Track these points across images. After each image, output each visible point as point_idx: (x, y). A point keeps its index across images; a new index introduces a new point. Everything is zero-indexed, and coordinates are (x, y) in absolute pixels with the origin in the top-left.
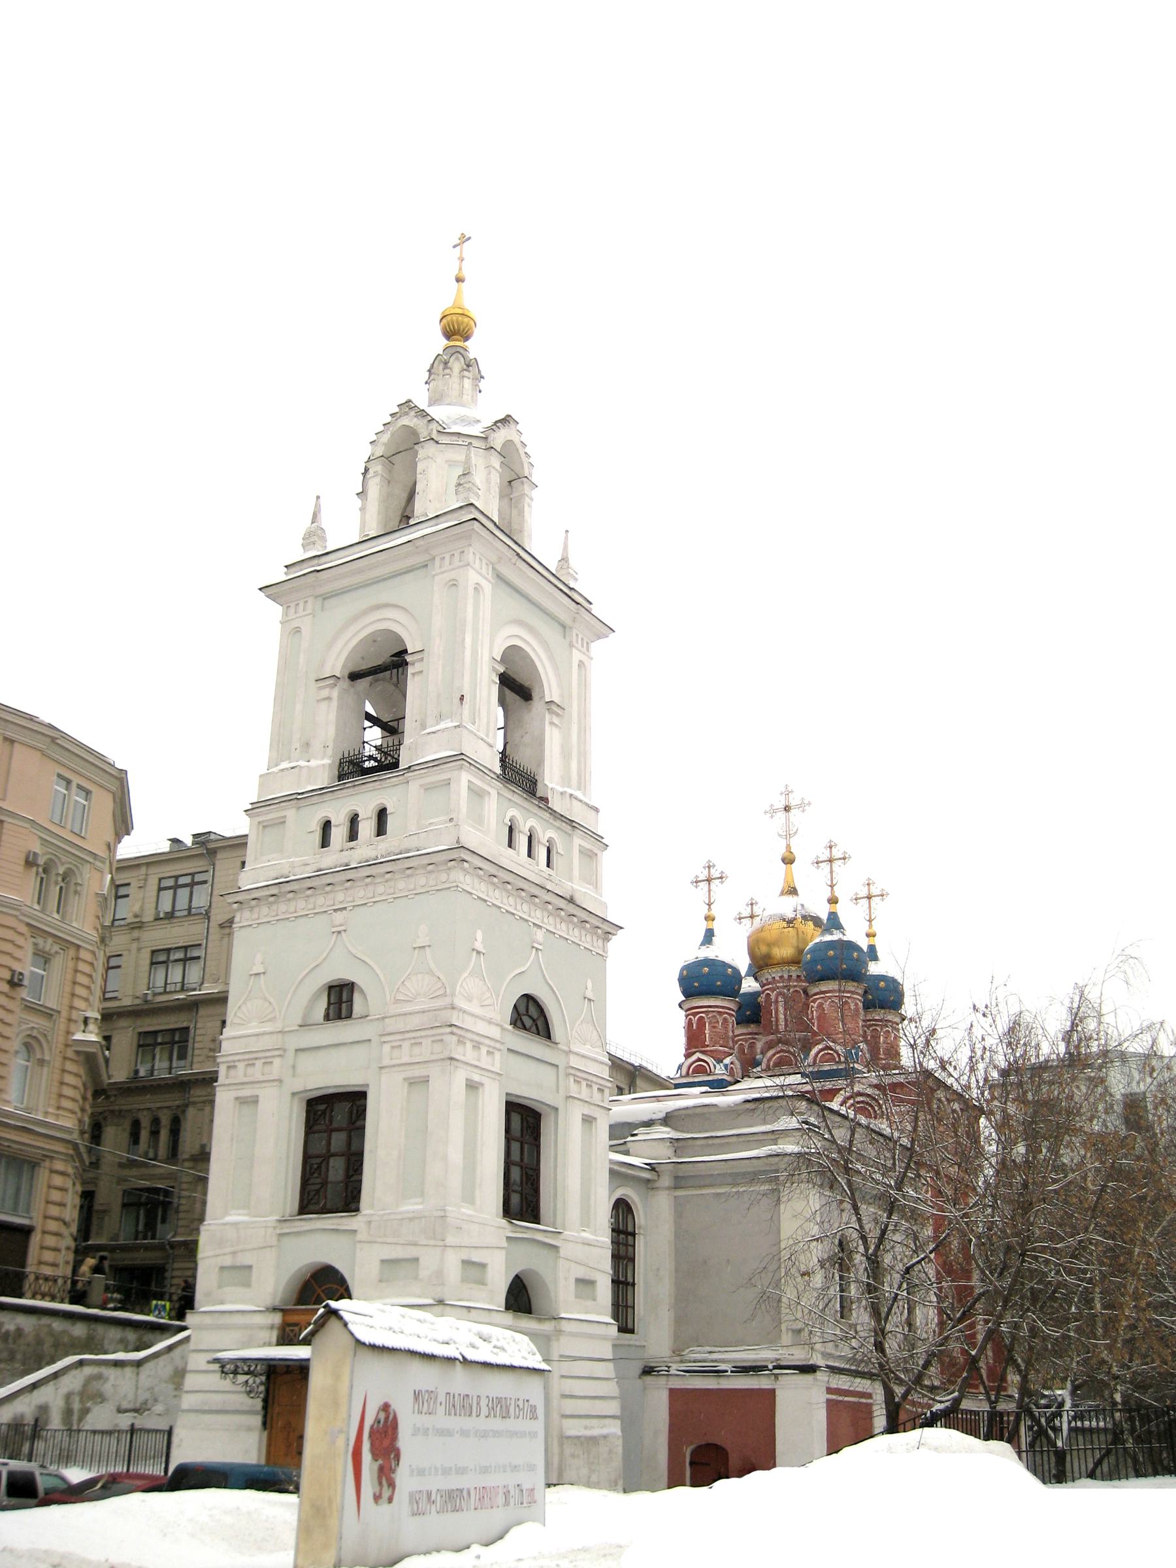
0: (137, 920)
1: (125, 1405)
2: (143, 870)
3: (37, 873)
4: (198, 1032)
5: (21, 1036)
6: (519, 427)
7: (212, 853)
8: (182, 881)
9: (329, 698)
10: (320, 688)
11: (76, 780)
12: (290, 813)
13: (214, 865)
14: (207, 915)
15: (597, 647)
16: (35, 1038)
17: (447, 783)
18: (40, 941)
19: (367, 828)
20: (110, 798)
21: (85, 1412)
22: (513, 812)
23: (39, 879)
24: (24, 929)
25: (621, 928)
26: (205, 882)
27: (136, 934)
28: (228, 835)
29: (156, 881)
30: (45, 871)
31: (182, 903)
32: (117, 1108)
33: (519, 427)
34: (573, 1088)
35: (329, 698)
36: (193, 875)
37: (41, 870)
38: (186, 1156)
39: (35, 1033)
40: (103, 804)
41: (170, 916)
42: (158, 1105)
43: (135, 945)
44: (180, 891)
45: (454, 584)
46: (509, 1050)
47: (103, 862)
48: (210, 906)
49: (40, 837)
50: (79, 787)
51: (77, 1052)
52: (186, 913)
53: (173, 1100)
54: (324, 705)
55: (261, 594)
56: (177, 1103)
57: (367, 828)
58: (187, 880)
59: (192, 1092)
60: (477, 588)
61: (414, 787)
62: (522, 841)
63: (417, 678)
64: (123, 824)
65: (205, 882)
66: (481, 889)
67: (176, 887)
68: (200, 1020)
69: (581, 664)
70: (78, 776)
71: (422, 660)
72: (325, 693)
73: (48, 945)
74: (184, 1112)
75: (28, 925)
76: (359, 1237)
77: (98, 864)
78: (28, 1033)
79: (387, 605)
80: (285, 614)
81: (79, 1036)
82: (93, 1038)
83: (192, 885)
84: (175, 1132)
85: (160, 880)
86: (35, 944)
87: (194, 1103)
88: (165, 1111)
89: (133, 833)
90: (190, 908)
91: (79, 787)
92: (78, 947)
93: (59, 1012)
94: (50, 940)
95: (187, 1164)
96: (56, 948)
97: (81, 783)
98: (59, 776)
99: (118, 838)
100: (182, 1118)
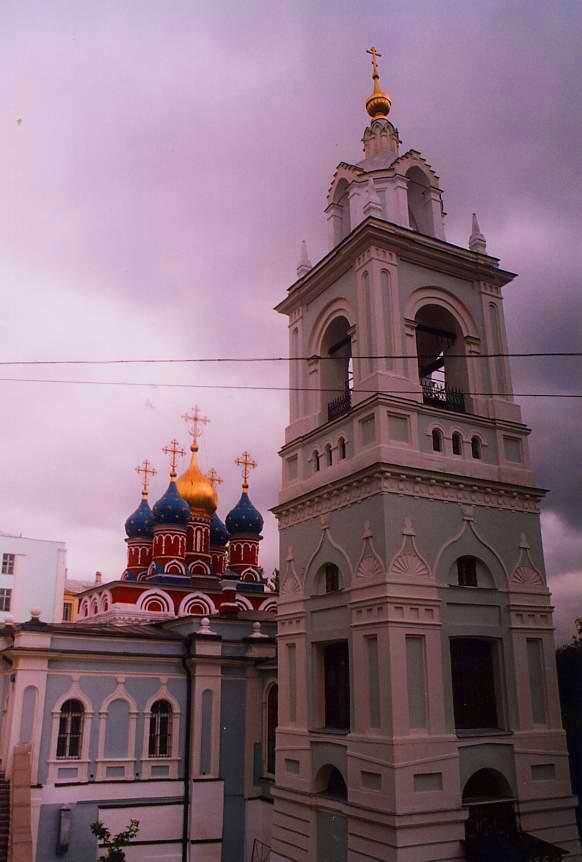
9: (316, 371)
10: (310, 365)
12: (299, 452)
15: (505, 290)
17: (372, 417)
19: (336, 454)
22: (435, 424)
34: (516, 624)
35: (316, 371)
45: (366, 274)
46: (448, 604)
54: (314, 375)
55: (275, 311)
57: (336, 454)
60: (385, 271)
61: (356, 423)
62: (448, 445)
63: (355, 344)
66: (407, 488)
69: (492, 305)
71: (354, 333)
72: (313, 368)
76: (348, 751)
79: (335, 301)
80: (291, 320)
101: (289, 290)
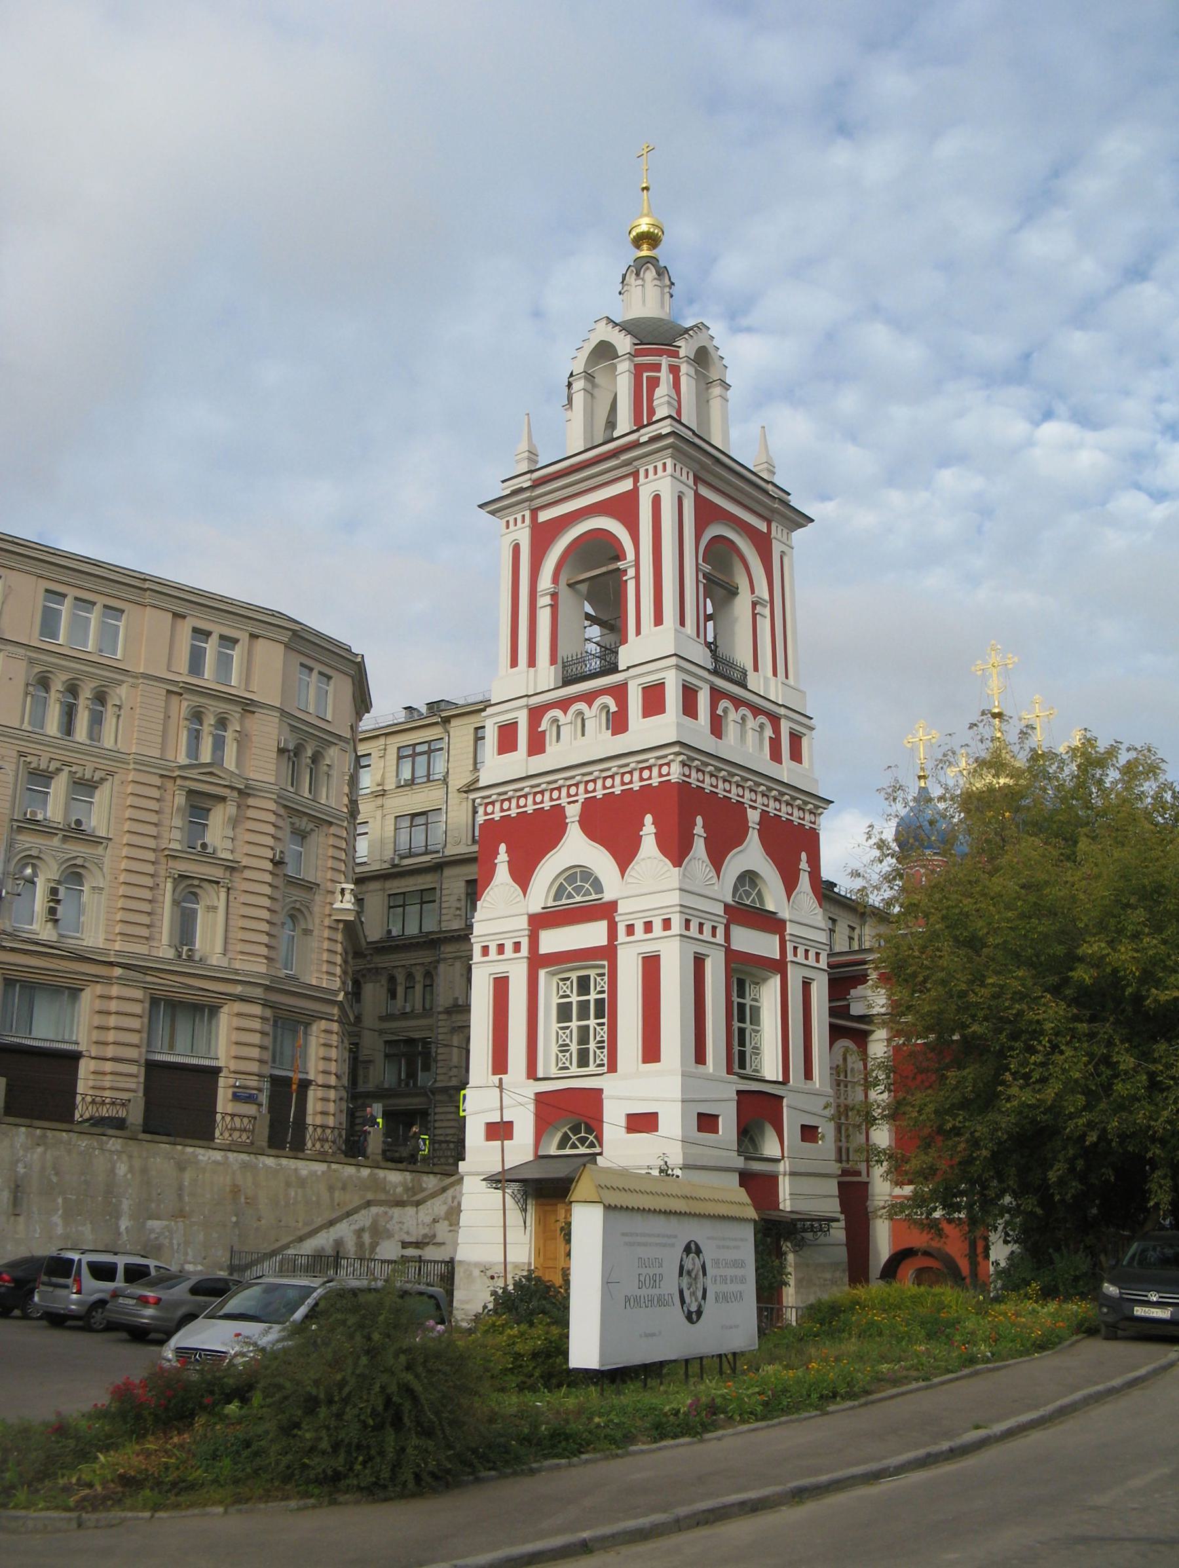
0: (380, 788)
1: (408, 1239)
2: (382, 741)
3: (289, 758)
4: (444, 892)
5: (285, 910)
6: (710, 332)
7: (446, 721)
8: (419, 749)
11: (318, 667)
13: (448, 732)
14: (445, 781)
15: (798, 535)
16: (299, 909)
18: (296, 820)
20: (350, 680)
21: (374, 1246)
23: (291, 764)
24: (282, 811)
25: (832, 802)
26: (441, 749)
27: (379, 801)
28: (461, 702)
29: (395, 751)
30: (295, 755)
31: (421, 771)
32: (372, 965)
33: (710, 332)
36: (429, 742)
37: (292, 754)
38: (440, 1009)
39: (298, 905)
40: (341, 688)
41: (412, 783)
42: (413, 962)
43: (379, 813)
44: (418, 759)
47: (348, 743)
48: (448, 772)
49: (289, 724)
50: (320, 673)
51: (338, 921)
52: (425, 779)
53: (425, 957)
56: (429, 960)
58: (425, 748)
59: (442, 949)
64: (362, 702)
65: (441, 749)
67: (414, 755)
68: (444, 881)
70: (320, 664)
73: (304, 824)
74: (436, 968)
75: (285, 807)
77: (341, 743)
78: (293, 905)
81: (337, 905)
82: (349, 906)
83: (429, 752)
84: (429, 986)
85: (399, 748)
86: (292, 824)
87: (445, 959)
88: (418, 967)
89: (372, 711)
90: (428, 775)
91: (320, 673)
92: (331, 823)
93: (318, 885)
94: (305, 819)
95: (441, 1017)
96: (311, 826)
97: (322, 670)
98: (302, 665)
99: (359, 716)
100: (434, 973)
101: (503, 482)
